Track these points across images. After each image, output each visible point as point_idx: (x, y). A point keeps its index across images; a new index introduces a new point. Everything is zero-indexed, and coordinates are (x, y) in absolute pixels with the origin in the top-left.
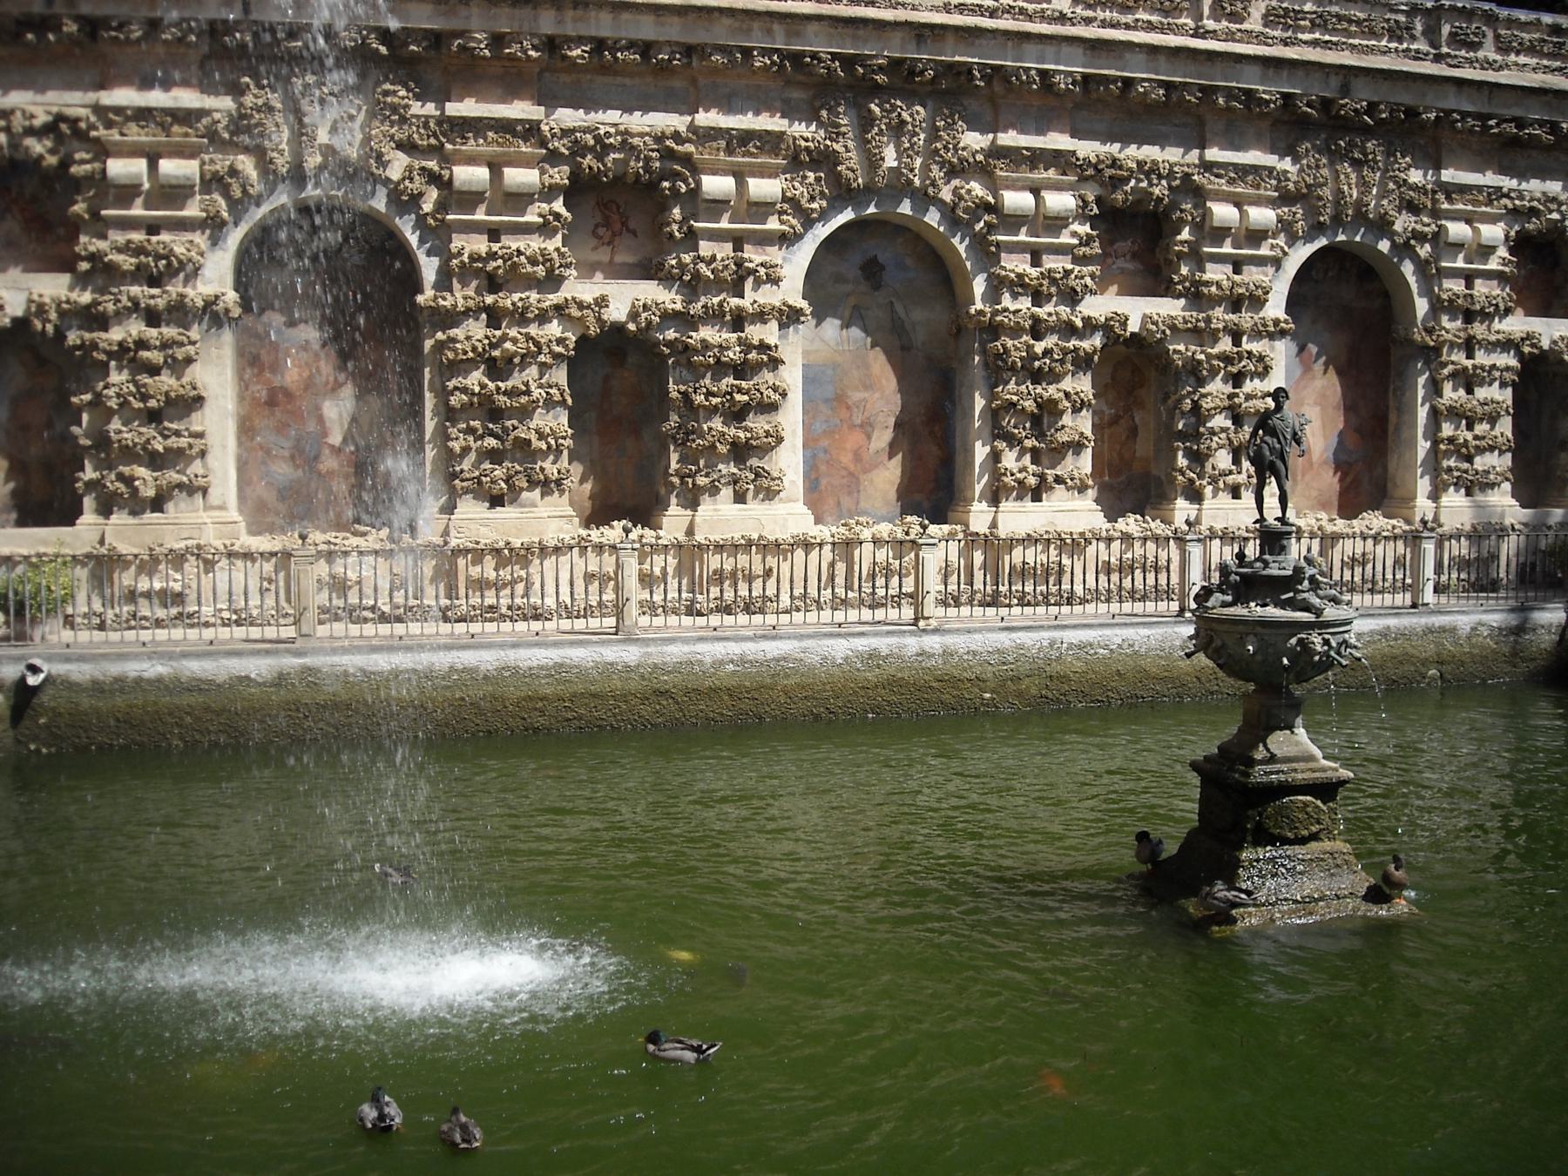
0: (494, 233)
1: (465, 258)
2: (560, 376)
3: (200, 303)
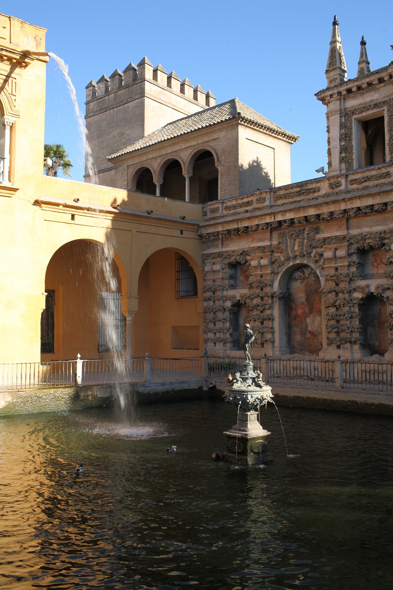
0: (337, 269)
1: (328, 277)
2: (357, 310)
3: (270, 294)
